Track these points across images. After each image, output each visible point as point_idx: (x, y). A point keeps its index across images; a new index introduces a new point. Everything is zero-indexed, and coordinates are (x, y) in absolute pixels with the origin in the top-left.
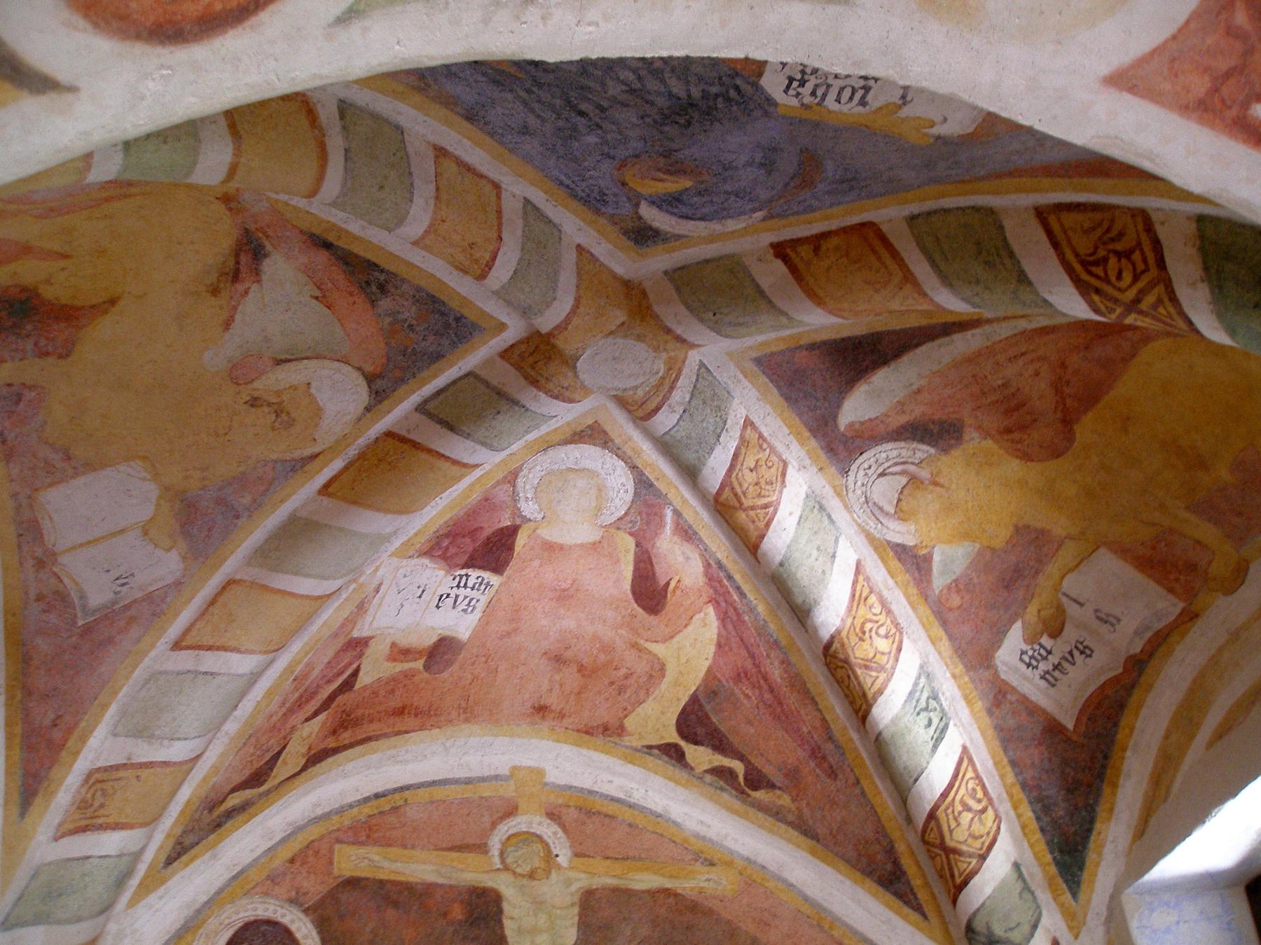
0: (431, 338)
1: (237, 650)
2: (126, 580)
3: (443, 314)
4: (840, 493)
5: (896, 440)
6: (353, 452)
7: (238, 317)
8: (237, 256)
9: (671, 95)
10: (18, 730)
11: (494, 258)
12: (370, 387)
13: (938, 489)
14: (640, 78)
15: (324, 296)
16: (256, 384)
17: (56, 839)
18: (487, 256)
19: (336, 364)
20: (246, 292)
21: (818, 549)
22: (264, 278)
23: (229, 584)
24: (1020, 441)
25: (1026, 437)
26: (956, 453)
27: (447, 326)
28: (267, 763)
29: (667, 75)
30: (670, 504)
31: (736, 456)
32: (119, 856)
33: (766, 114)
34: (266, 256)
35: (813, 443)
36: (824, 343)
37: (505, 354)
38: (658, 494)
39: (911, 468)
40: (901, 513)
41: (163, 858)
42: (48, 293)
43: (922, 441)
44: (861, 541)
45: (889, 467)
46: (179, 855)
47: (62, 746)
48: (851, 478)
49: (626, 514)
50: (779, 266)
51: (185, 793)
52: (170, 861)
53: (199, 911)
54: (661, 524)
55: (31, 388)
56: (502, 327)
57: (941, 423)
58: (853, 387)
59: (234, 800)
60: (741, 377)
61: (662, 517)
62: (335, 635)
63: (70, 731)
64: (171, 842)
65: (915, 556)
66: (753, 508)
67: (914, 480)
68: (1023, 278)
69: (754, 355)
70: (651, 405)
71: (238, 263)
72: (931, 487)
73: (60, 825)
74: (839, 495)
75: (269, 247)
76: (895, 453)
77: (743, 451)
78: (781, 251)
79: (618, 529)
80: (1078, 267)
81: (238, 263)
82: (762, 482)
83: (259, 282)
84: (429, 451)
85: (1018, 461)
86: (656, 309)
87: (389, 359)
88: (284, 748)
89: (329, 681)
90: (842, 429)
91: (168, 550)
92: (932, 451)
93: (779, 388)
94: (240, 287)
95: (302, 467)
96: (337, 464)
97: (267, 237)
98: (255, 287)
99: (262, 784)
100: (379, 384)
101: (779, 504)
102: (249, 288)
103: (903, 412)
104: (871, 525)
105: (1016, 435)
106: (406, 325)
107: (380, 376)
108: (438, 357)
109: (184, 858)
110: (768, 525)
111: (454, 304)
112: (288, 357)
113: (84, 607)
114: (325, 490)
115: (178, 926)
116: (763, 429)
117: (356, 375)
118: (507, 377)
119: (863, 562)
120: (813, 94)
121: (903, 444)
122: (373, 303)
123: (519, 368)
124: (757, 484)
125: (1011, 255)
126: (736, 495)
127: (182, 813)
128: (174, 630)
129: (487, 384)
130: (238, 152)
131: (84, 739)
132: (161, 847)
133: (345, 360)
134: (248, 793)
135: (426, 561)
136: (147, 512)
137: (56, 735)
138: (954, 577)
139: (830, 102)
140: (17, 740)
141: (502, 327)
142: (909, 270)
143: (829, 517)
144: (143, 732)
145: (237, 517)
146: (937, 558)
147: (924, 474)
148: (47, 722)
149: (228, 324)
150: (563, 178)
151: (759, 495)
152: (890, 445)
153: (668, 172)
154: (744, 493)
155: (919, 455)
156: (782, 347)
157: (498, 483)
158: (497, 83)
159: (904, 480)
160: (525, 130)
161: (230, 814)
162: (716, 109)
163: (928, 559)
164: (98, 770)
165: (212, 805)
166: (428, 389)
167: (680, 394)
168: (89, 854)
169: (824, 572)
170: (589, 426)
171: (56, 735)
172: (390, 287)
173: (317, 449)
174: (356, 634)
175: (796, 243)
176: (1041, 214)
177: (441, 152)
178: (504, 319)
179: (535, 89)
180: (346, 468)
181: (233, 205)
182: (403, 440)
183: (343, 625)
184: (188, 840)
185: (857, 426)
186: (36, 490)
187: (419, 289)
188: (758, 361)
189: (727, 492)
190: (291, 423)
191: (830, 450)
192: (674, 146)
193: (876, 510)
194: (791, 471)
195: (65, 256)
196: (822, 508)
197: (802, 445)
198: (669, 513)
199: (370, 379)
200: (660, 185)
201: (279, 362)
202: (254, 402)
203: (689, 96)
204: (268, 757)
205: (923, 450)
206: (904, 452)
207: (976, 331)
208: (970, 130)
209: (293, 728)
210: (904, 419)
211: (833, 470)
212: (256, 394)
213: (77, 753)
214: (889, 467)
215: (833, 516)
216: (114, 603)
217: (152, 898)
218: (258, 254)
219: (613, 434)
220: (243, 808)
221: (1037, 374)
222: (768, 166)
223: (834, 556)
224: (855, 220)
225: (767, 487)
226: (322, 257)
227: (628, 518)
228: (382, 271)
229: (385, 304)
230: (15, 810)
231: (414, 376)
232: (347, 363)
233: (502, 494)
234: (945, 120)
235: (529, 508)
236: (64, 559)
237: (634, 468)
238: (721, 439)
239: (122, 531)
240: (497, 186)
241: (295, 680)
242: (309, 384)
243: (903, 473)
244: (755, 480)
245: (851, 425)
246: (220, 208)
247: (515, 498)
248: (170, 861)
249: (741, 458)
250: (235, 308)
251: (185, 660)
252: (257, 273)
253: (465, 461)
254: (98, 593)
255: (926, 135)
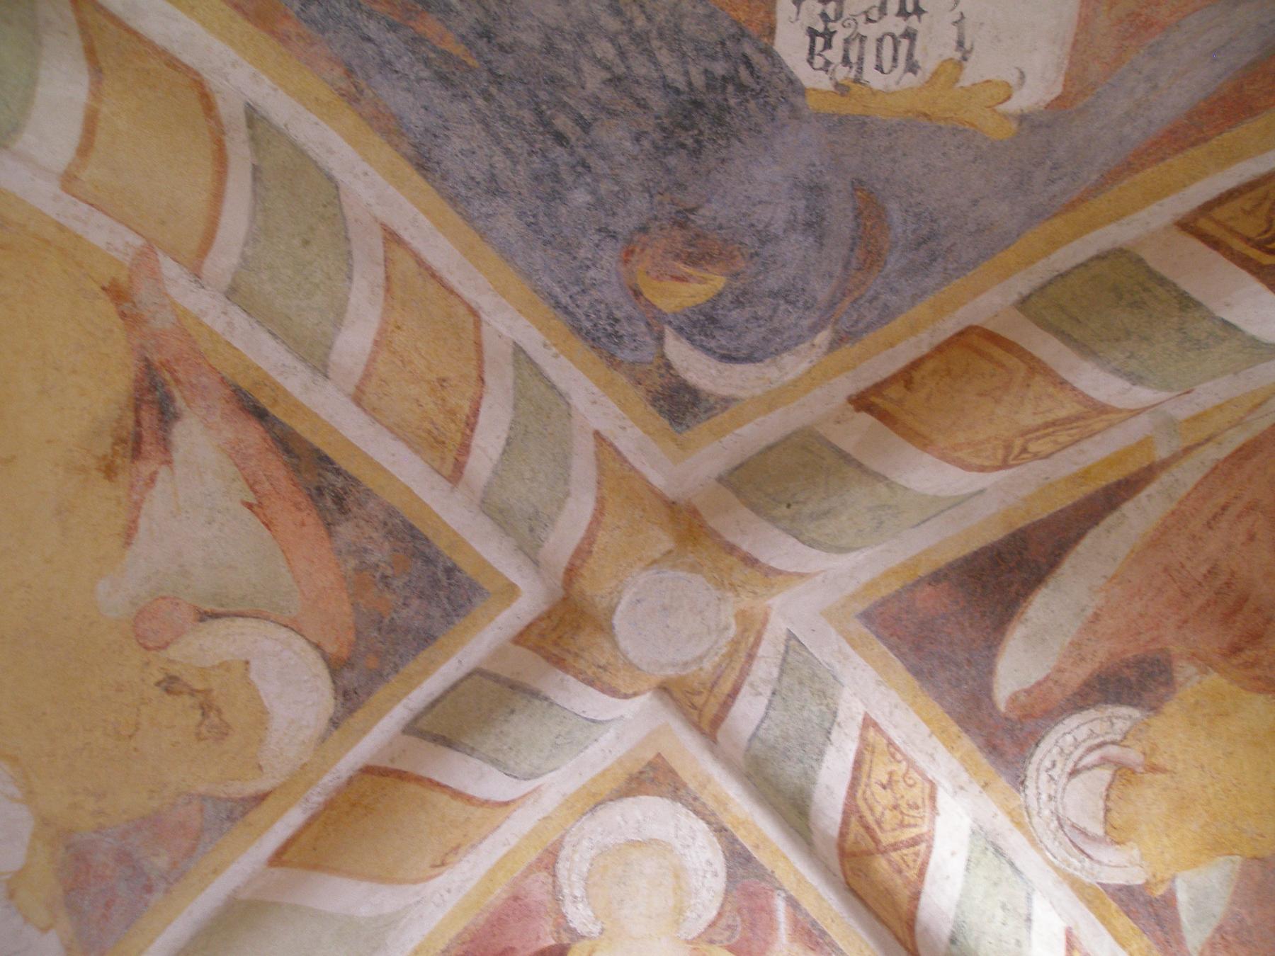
0: (415, 603)
3: (428, 561)
4: (1020, 820)
5: (1081, 708)
6: (316, 797)
7: (143, 523)
8: (137, 409)
9: (667, 87)
11: (476, 412)
12: (334, 682)
13: (1160, 777)
14: (622, 54)
15: (260, 505)
16: (172, 652)
18: (466, 407)
19: (284, 633)
20: (152, 479)
21: (1004, 907)
22: (177, 456)
24: (1255, 664)
25: (1263, 653)
26: (1171, 708)
27: (435, 583)
29: (656, 43)
30: (781, 888)
31: (858, 764)
33: (795, 112)
34: (177, 417)
35: (967, 743)
36: (951, 566)
37: (521, 638)
38: (763, 874)
39: (1113, 751)
40: (1115, 834)
43: (1118, 700)
44: (1065, 895)
45: (1081, 758)
48: (1031, 790)
49: (720, 915)
50: (866, 419)
54: (772, 926)
56: (511, 591)
57: (1139, 663)
58: (1003, 634)
60: (848, 649)
61: (771, 913)
65: (1150, 902)
66: (895, 847)
67: (1123, 774)
68: (1186, 303)
69: (861, 607)
70: (726, 687)
71: (138, 423)
72: (1148, 777)
74: (1019, 824)
75: (180, 403)
76: (1084, 731)
77: (867, 756)
78: (862, 402)
79: (711, 942)
80: (1254, 253)
81: (138, 423)
82: (903, 803)
83: (169, 462)
84: (419, 780)
85: (1261, 698)
86: (712, 523)
87: (358, 633)
90: (1002, 707)
91: (45, 930)
92: (1136, 713)
93: (901, 656)
94: (145, 468)
95: (244, 814)
96: (295, 818)
97: (177, 381)
98: (163, 472)
100: (350, 678)
101: (932, 838)
102: (155, 473)
103: (1083, 659)
104: (1076, 865)
105: (1249, 655)
106: (378, 575)
107: (348, 663)
108: (426, 639)
110: (922, 873)
111: (441, 544)
112: (220, 610)
114: (279, 858)
116: (892, 733)
117: (312, 656)
118: (526, 665)
119: (1075, 932)
120: (846, 61)
121: (1092, 713)
122: (329, 526)
123: (536, 649)
124: (895, 807)
125: (1162, 281)
126: (867, 828)
129: (496, 678)
130: (96, 93)
133: (293, 626)
138: (1215, 923)
139: (870, 75)
141: (511, 591)
142: (1033, 358)
143: (1012, 864)
145: (149, 889)
146: (1182, 897)
147: (1133, 756)
149: (129, 534)
150: (557, 290)
151: (902, 825)
152: (1073, 721)
153: (692, 260)
154: (879, 823)
155: (1120, 725)
156: (896, 585)
157: (530, 869)
158: (444, 79)
159: (1106, 774)
160: (494, 188)
162: (729, 109)
163: (1169, 901)
166: (420, 696)
167: (765, 668)
169: (1018, 943)
170: (650, 764)
172: (350, 501)
173: (264, 785)
175: (879, 388)
176: (1187, 225)
177: (392, 237)
178: (514, 577)
179: (493, 90)
180: (308, 824)
181: (126, 306)
182: (384, 772)
185: (1022, 698)
187: (391, 512)
188: (867, 617)
189: (855, 826)
190: (223, 732)
191: (992, 748)
192: (690, 202)
193: (1077, 837)
194: (943, 798)
196: (998, 851)
197: (951, 749)
198: (780, 906)
199: (336, 667)
200: (683, 288)
201: (205, 616)
202: (171, 685)
203: (690, 84)
205: (1123, 716)
206: (1098, 727)
207: (1152, 489)
208: (1058, 90)
210: (1081, 673)
211: (1002, 783)
212: (174, 670)
214: (1081, 758)
215: (1018, 864)
218: (166, 415)
219: (685, 775)
221: (1252, 537)
222: (815, 225)
223: (1029, 920)
224: (949, 327)
225: (913, 813)
226: (253, 434)
227: (723, 922)
228: (338, 472)
229: (346, 531)
231: (396, 669)
232: (299, 632)
233: (537, 889)
234: (1022, 76)
235: (579, 916)
237: (721, 831)
238: (834, 736)
240: (474, 313)
242: (247, 663)
243: (1104, 761)
244: (892, 802)
245: (1014, 699)
246: (106, 306)
247: (556, 893)
249: (866, 768)
250: (137, 506)
252: (165, 445)
253: (470, 792)
255: (1005, 116)
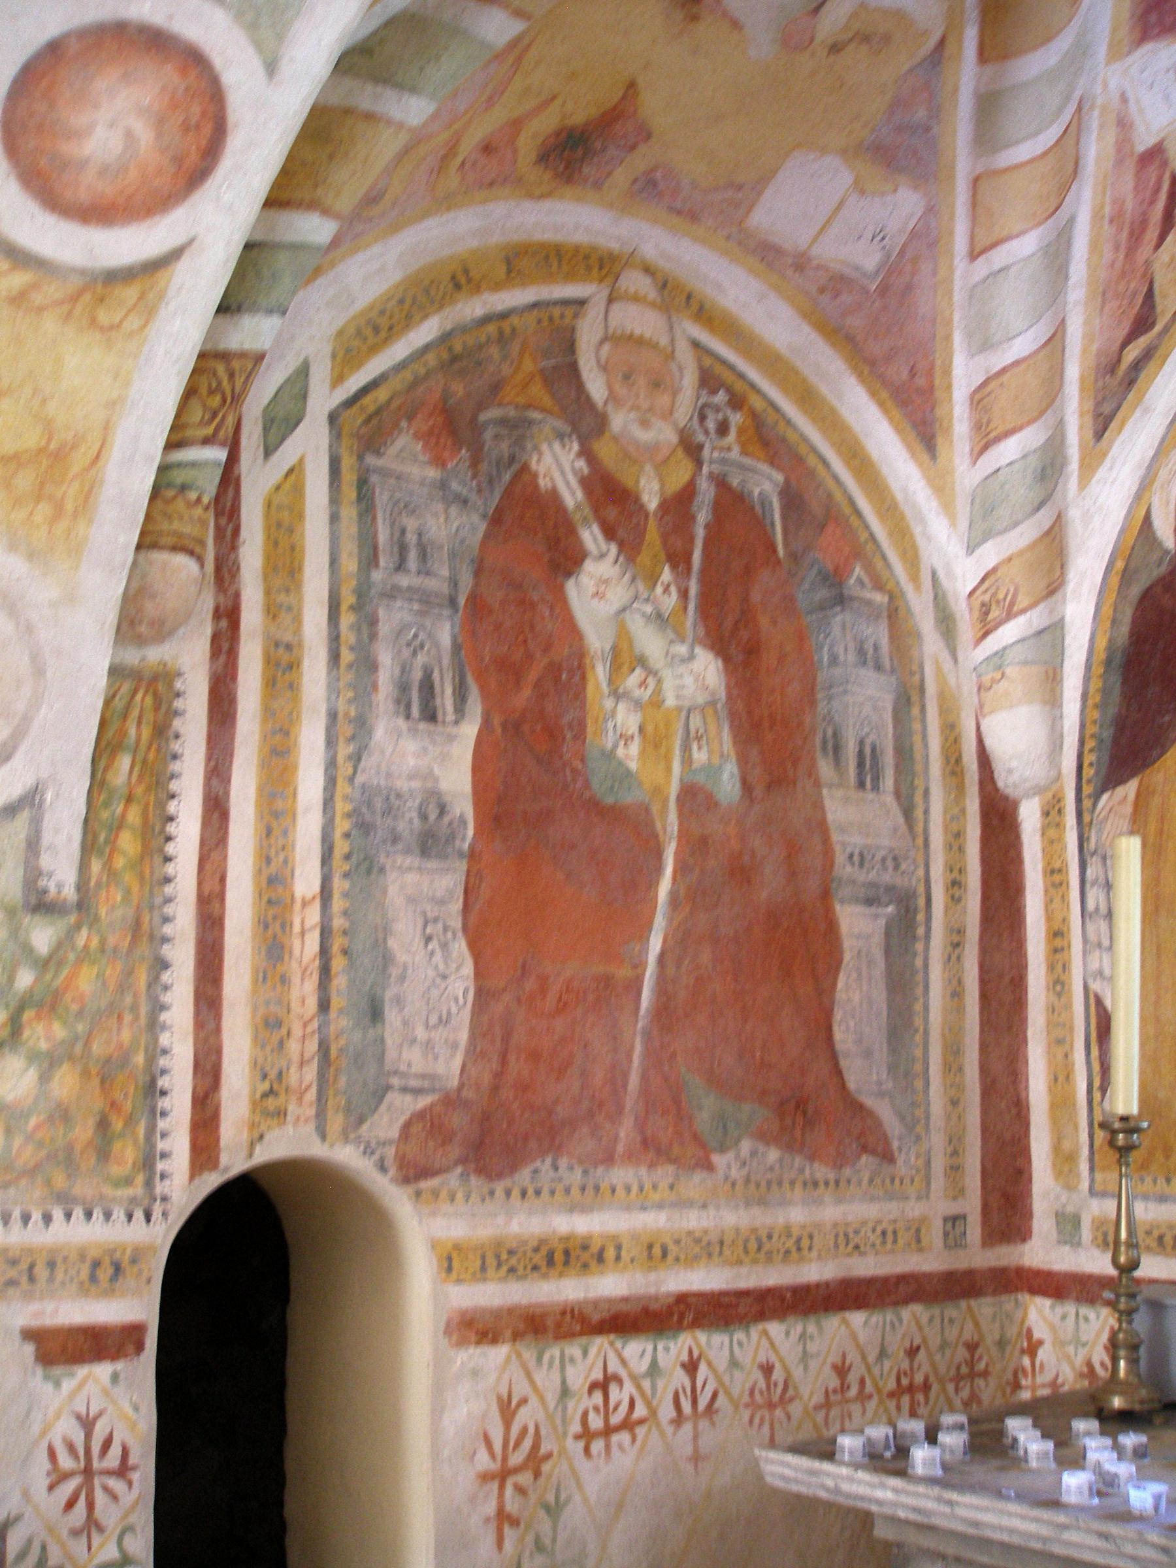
1: (1009, 238)
2: (881, 235)
10: (884, 395)
16: (820, 36)
17: (975, 463)
23: (976, 181)
28: (1144, 303)
32: (1024, 457)
41: (1089, 434)
42: (579, 118)
46: (1105, 429)
47: (931, 388)
51: (1073, 372)
52: (1099, 434)
53: (1150, 467)
55: (654, 169)
59: (1132, 353)
62: (1119, 162)
63: (930, 372)
64: (1089, 420)
73: (972, 450)
88: (1151, 283)
89: (1152, 202)
91: (895, 190)
99: (1153, 324)
109: (1113, 426)
113: (865, 274)
114: (983, 57)
115: (1135, 488)
127: (1082, 389)
128: (961, 243)
131: (947, 372)
132: (1081, 428)
134: (1143, 342)
135: (1149, 47)
136: (846, 178)
137: (921, 381)
140: (889, 403)
144: (985, 345)
145: (928, 129)
148: (905, 375)
149: (736, 25)
161: (1138, 366)
164: (975, 392)
165: (1112, 368)
168: (998, 466)
171: (921, 381)
174: (1141, 148)
183: (1119, 150)
184: (1107, 408)
186: (740, 223)
195: (554, 98)
202: (835, 48)
204: (1139, 300)
209: (1148, 263)
213: (949, 387)
216: (888, 256)
217: (1102, 473)
220: (1147, 355)
230: (925, 457)
236: (815, 251)
239: (841, 205)
241: (1111, 221)
248: (1099, 434)
251: (981, 268)
254: (868, 259)
